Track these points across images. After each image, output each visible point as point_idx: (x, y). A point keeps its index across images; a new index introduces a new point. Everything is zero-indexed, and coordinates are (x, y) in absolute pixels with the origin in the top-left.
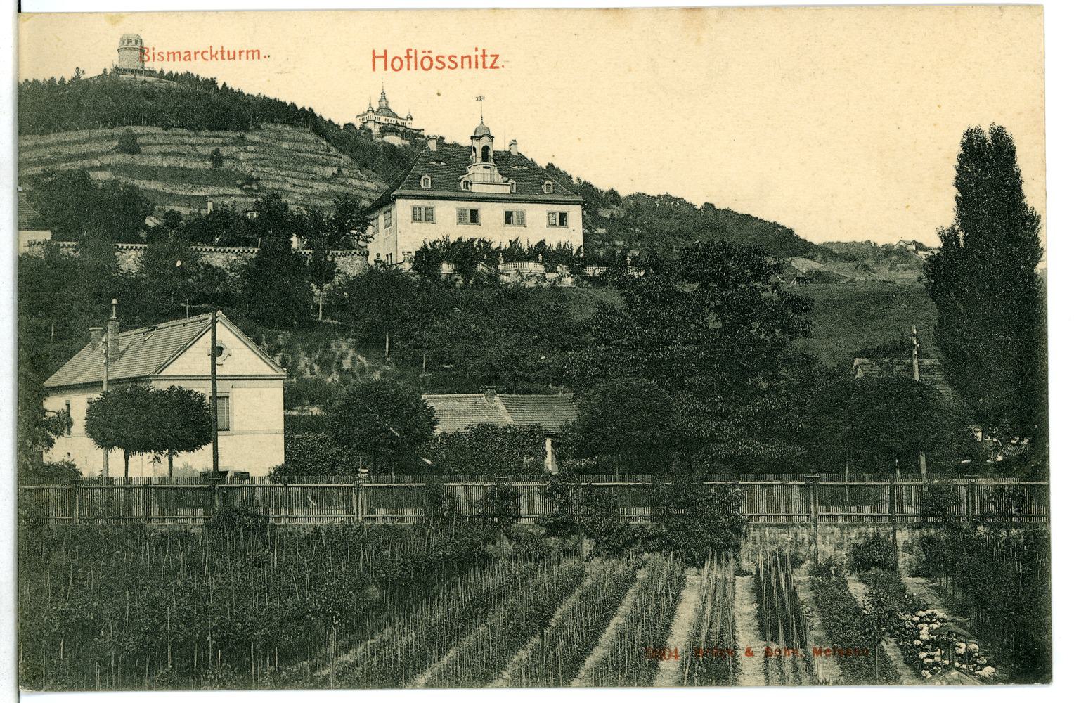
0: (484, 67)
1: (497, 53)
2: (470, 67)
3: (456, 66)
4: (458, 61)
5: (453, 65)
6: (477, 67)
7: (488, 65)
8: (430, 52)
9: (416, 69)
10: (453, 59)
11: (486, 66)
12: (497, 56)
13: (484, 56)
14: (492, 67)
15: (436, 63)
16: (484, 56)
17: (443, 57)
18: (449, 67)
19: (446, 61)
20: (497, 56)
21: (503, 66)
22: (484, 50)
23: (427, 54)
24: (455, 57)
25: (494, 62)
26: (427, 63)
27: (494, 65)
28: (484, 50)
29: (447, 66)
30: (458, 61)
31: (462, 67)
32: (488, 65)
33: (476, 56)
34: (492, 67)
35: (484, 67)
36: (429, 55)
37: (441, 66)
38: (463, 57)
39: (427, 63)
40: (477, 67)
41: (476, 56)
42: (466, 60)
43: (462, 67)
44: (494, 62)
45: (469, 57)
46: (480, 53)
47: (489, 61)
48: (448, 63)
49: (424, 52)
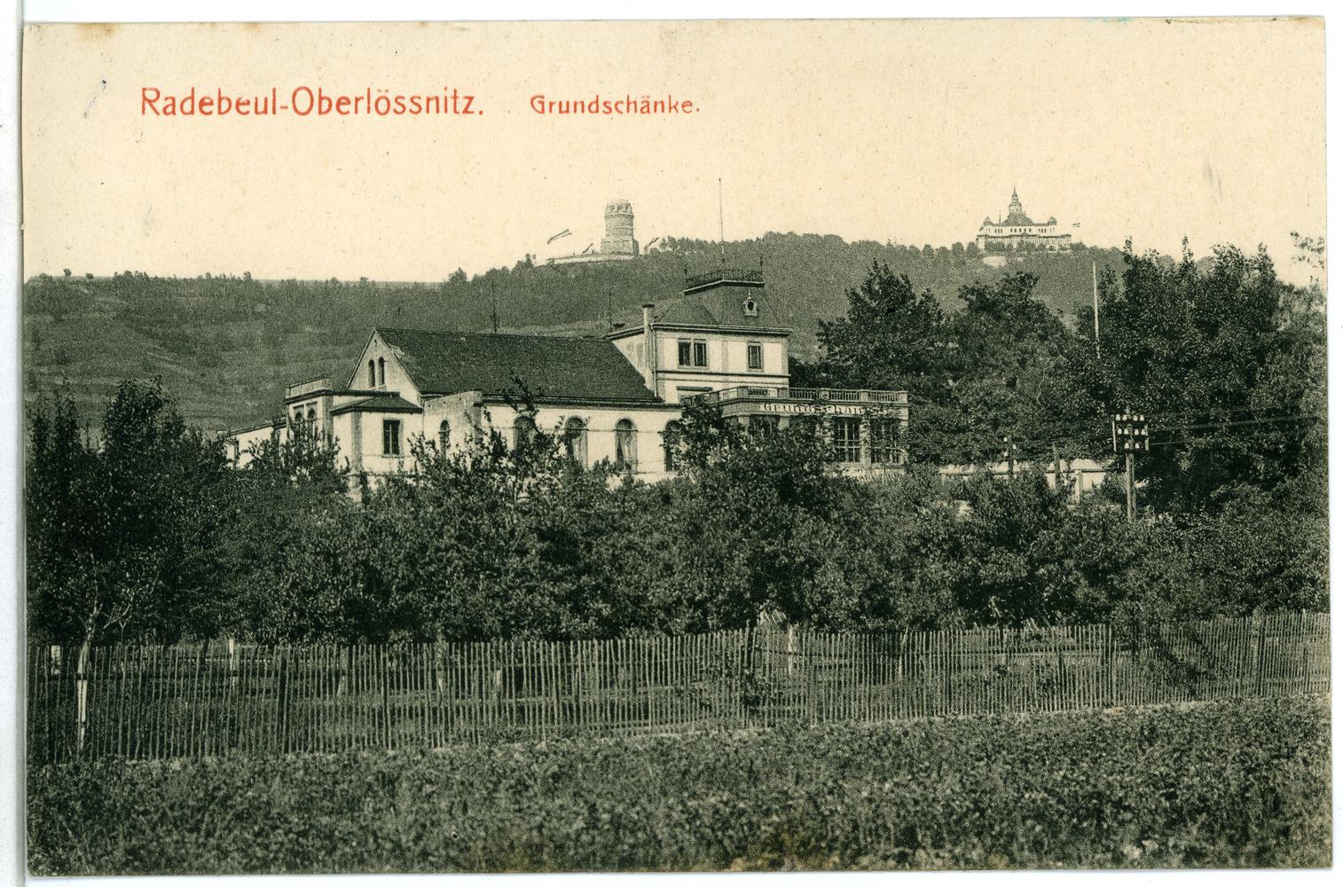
0: (456, 112)
1: (469, 95)
2: (438, 111)
3: (420, 109)
4: (423, 103)
5: (415, 109)
6: (446, 111)
7: (460, 108)
8: (387, 91)
9: (369, 112)
10: (416, 100)
11: (458, 109)
12: (471, 99)
13: (455, 97)
14: (466, 111)
15: (393, 104)
16: (455, 97)
17: (403, 98)
18: (411, 111)
19: (407, 103)
20: (471, 99)
21: (481, 113)
22: (455, 91)
23: (383, 94)
24: (419, 98)
25: (469, 104)
26: (383, 106)
27: (469, 110)
28: (455, 91)
29: (407, 110)
30: (423, 103)
31: (428, 111)
32: (460, 108)
33: (446, 98)
34: (466, 111)
35: (456, 112)
36: (388, 95)
37: (400, 109)
38: (428, 100)
39: (383, 106)
40: (446, 111)
41: (446, 98)
42: (433, 104)
43: (428, 111)
44: (469, 104)
45: (437, 99)
46: (450, 93)
47: (461, 106)
48: (409, 106)
49: (379, 91)
